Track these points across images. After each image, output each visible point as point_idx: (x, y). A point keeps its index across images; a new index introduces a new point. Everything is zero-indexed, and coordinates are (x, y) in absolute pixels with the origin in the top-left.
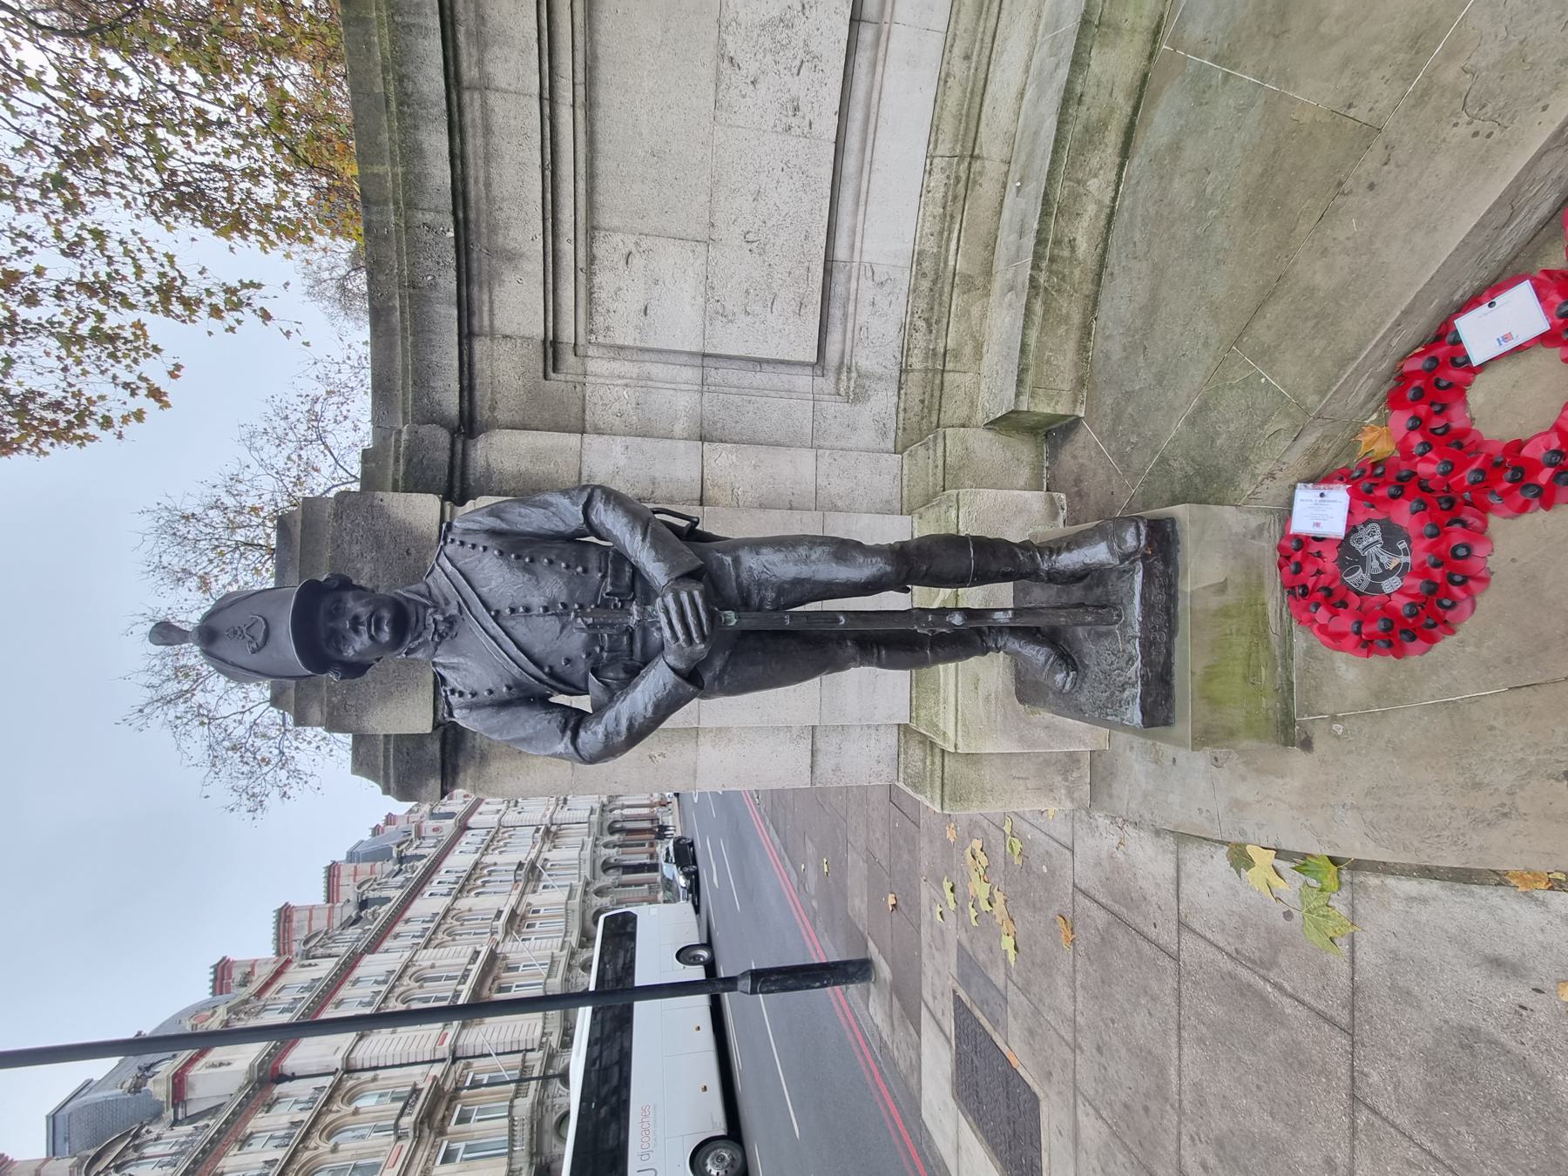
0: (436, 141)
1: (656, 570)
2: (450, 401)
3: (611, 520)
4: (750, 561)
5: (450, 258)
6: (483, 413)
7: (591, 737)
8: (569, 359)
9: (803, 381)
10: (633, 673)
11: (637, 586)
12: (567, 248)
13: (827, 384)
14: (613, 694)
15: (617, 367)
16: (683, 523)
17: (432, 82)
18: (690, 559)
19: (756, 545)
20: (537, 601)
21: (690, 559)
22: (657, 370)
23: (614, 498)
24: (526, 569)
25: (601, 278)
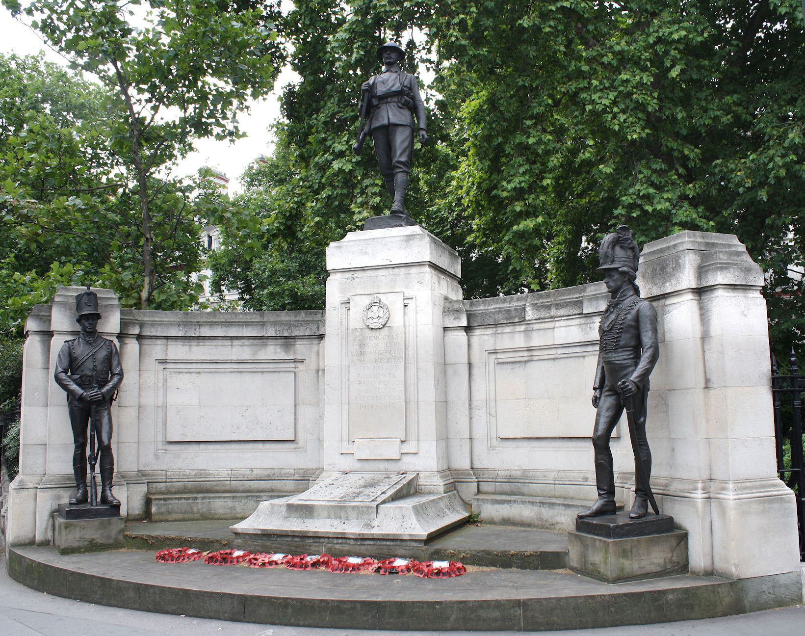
0: (219, 332)
1: (105, 390)
2: (146, 333)
3: (116, 379)
4: (106, 413)
5: (188, 335)
6: (146, 342)
7: (63, 376)
8: (162, 366)
9: (160, 438)
10: (79, 385)
11: (101, 386)
12: (194, 366)
13: (160, 446)
14: (75, 381)
15: (161, 380)
16: (114, 398)
17: (233, 332)
18: (108, 398)
19: (109, 414)
20: (96, 363)
21: (108, 398)
22: (161, 392)
23: (120, 380)
24: (104, 361)
25: (186, 376)
